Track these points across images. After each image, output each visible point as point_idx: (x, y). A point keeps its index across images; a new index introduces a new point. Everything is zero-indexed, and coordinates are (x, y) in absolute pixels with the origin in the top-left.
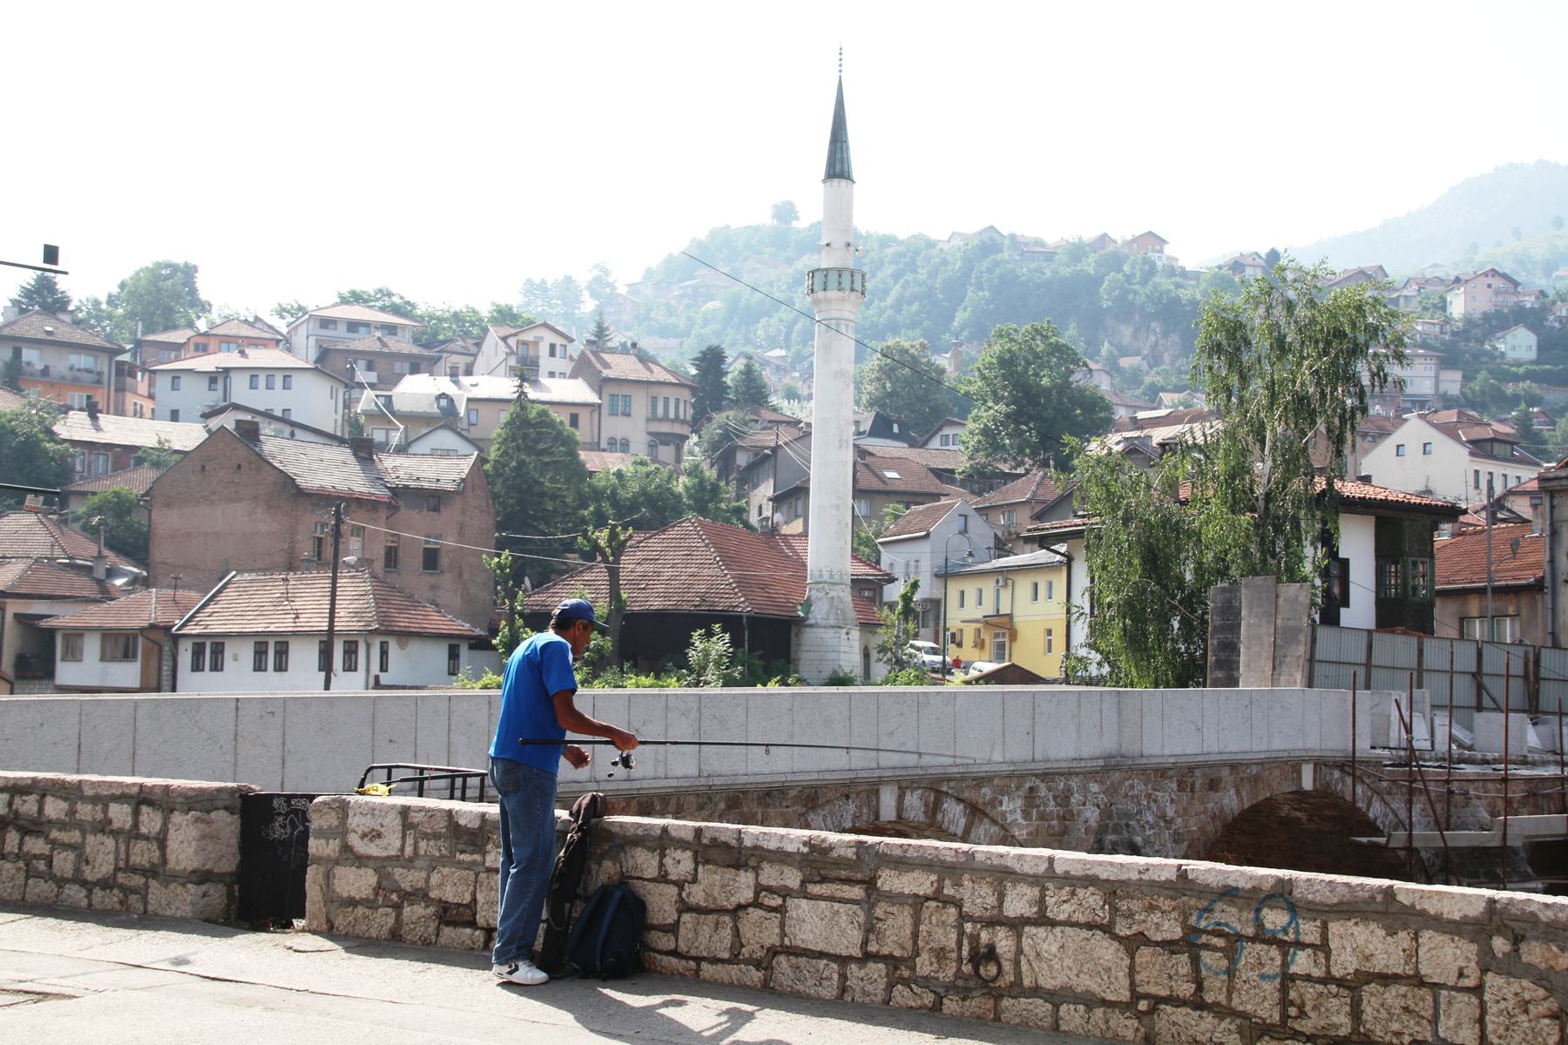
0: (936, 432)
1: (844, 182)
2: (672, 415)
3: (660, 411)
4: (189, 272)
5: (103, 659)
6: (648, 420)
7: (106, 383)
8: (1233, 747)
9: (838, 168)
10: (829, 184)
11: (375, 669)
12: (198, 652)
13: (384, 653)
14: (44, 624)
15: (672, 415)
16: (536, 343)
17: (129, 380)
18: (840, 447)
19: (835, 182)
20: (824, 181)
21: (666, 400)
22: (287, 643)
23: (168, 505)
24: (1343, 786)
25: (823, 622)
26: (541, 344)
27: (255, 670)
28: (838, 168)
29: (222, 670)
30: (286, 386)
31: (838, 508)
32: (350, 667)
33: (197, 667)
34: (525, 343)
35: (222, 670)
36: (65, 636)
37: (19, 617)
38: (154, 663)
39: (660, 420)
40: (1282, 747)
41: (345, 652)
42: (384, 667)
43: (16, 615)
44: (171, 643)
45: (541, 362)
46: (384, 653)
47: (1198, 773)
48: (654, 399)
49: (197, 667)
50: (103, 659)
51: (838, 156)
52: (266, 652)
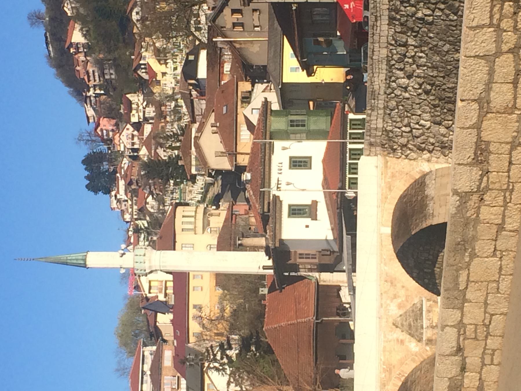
2: (192, 220)
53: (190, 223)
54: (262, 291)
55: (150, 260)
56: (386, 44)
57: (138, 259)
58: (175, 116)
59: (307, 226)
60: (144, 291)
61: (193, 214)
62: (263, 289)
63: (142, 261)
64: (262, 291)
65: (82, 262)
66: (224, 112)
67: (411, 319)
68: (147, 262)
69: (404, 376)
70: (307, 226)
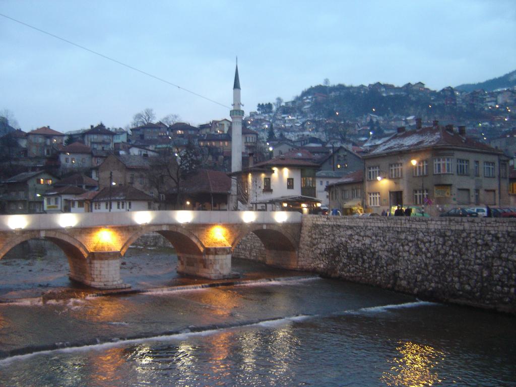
2: (251, 141)
4: (152, 110)
5: (79, 207)
9: (237, 86)
11: (128, 208)
12: (96, 205)
13: (130, 205)
23: (101, 172)
28: (237, 86)
32: (123, 208)
33: (96, 209)
42: (130, 207)
46: (130, 205)
48: (246, 138)
49: (96, 209)
50: (79, 207)
56: (366, 225)
58: (321, 114)
61: (251, 141)
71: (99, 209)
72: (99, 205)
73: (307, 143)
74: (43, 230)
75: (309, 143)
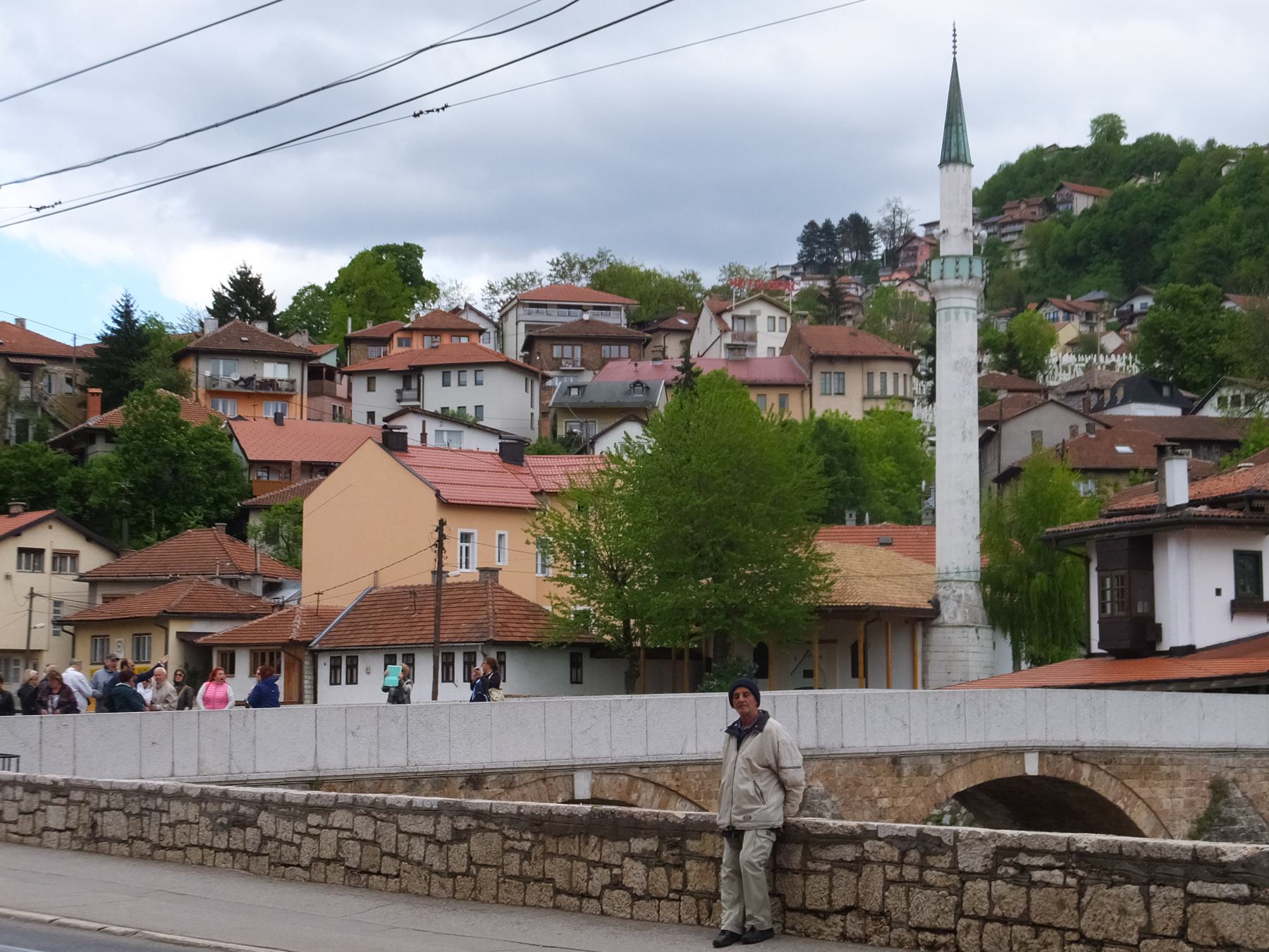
0: (1212, 394)
1: (959, 167)
3: (877, 388)
6: (865, 398)
7: (298, 390)
8: (946, 740)
10: (944, 169)
12: (335, 668)
14: (201, 640)
15: (890, 392)
16: (752, 318)
17: (326, 382)
18: (964, 439)
19: (951, 167)
20: (941, 166)
21: (884, 374)
22: (413, 655)
24: (1085, 775)
25: (950, 622)
26: (758, 318)
27: (331, 684)
29: (356, 683)
30: (478, 383)
31: (963, 502)
33: (334, 681)
34: (743, 318)
35: (356, 683)
36: (223, 655)
37: (181, 637)
38: (295, 677)
39: (877, 398)
40: (1001, 739)
41: (465, 663)
43: (178, 633)
44: (310, 658)
45: (759, 337)
47: (904, 761)
48: (870, 374)
49: (334, 681)
51: (954, 140)
52: (340, 667)
53: (884, 388)
54: (851, 516)
55: (961, 288)
57: (964, 265)
59: (1218, 592)
60: (736, 307)
61: (901, 393)
62: (854, 516)
63: (960, 272)
64: (851, 516)
65: (953, 154)
66: (1120, 449)
67: (1245, 825)
68: (958, 282)
69: (1126, 806)
70: (1218, 592)
71: (352, 680)
72: (352, 666)
73: (1113, 404)
74: (583, 768)
75: (1125, 401)
